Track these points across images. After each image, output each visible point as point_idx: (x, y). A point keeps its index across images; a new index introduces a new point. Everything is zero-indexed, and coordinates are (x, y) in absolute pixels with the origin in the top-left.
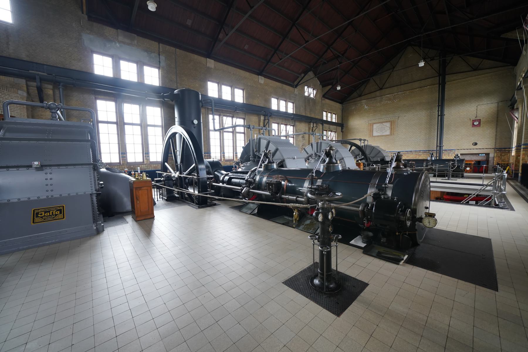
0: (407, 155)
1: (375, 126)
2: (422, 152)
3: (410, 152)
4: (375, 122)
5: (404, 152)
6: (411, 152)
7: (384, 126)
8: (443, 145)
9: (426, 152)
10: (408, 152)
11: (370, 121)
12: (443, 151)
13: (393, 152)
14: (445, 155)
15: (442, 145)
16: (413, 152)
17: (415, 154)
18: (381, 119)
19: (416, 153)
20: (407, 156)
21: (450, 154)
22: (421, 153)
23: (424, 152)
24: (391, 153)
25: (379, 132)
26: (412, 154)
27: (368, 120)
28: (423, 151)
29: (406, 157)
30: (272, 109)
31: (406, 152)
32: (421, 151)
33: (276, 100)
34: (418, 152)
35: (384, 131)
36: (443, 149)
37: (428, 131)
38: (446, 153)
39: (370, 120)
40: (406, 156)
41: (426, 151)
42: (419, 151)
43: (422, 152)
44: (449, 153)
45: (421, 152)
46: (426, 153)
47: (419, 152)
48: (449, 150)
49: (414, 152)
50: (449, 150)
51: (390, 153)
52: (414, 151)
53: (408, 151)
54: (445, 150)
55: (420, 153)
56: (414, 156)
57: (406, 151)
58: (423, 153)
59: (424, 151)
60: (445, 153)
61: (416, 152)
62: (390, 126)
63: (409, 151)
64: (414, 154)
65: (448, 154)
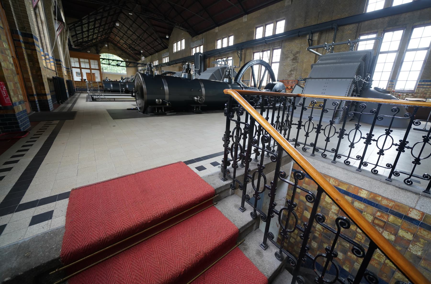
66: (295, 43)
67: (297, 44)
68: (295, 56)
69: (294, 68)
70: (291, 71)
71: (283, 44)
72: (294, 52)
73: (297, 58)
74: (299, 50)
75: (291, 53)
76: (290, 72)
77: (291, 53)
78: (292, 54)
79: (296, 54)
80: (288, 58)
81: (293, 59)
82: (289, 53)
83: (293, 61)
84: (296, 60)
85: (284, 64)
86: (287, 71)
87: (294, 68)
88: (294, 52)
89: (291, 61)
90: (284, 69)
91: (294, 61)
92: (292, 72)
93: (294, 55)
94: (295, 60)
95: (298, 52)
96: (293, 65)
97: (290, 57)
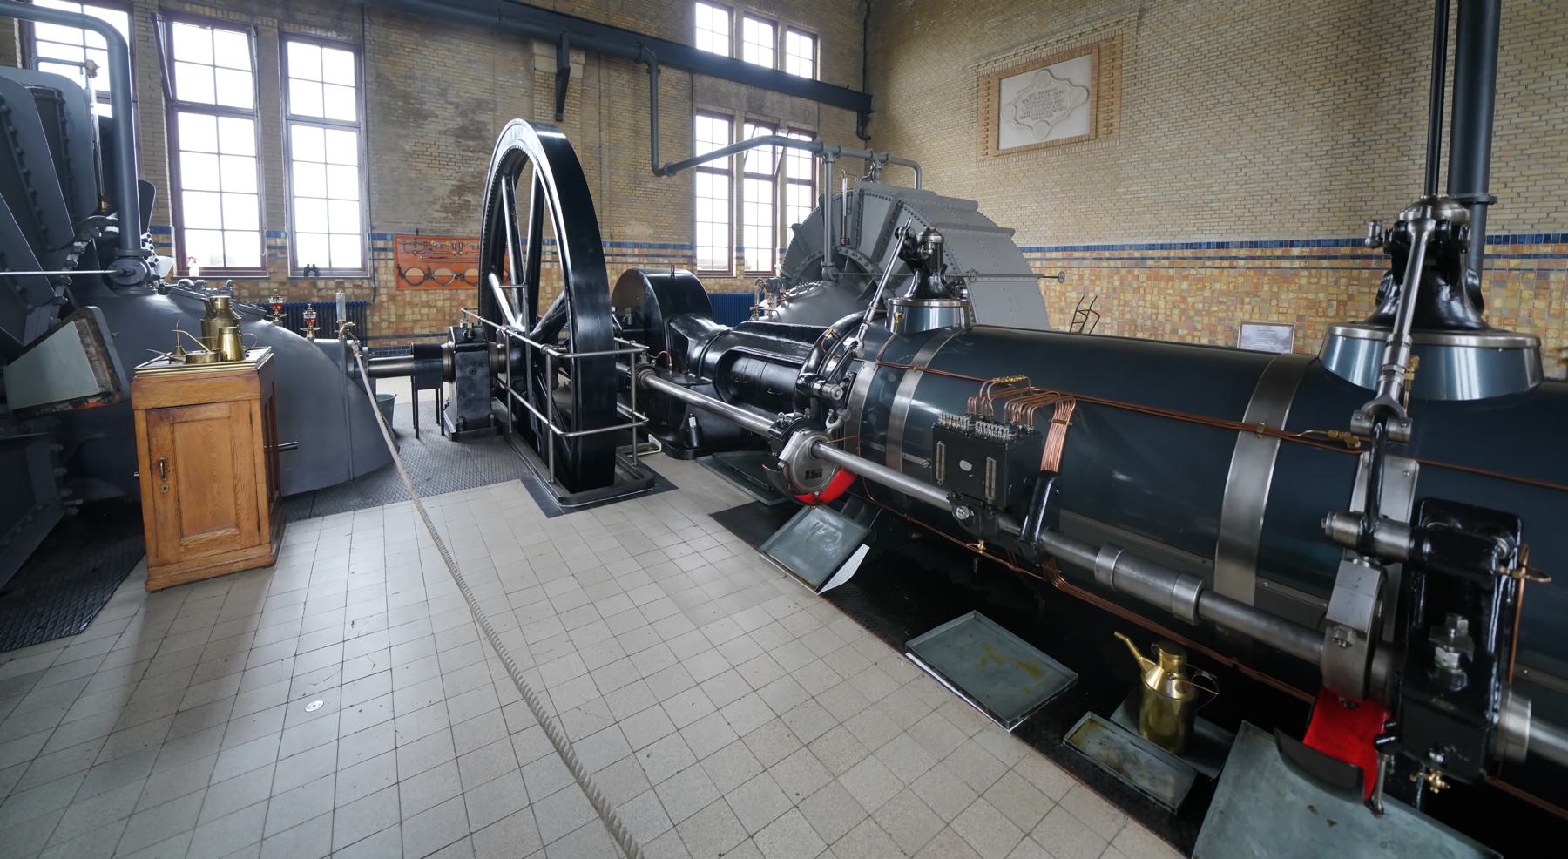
0: (1193, 272)
1: (1011, 89)
2: (1306, 252)
3: (1211, 252)
4: (1009, 63)
5: (1172, 253)
6: (1222, 252)
7: (1054, 84)
8: (1485, 189)
9: (1332, 251)
10: (1199, 253)
11: (982, 62)
12: (1488, 249)
13: (1105, 248)
14: (1500, 283)
15: (1479, 195)
16: (1234, 252)
17: (1251, 264)
18: (1038, 38)
19: (1259, 263)
20: (1201, 280)
21: (1553, 276)
22: (1297, 264)
23: (1316, 251)
24: (1095, 254)
25: (1032, 123)
26: (1226, 263)
27: (978, 54)
28: (1307, 243)
29: (1185, 286)
30: (786, 74)
31: (1188, 253)
32: (1291, 244)
33: (767, 29)
34: (1268, 252)
35: (1056, 114)
36: (1491, 231)
37: (1351, 85)
38: (1514, 263)
39: (984, 57)
40: (1185, 278)
41: (1337, 243)
42: (1281, 244)
43: (1306, 252)
44: (1551, 263)
45: (1296, 251)
46: (1336, 263)
47: (1278, 252)
48: (1547, 239)
49: (1243, 252)
50: (1547, 239)
51: (1087, 254)
52: (1241, 245)
53: (1198, 246)
54: (1506, 240)
55: (1286, 264)
56: (1241, 280)
57: (1187, 246)
58: (1314, 263)
59: (1319, 243)
60: (1499, 263)
61: (1259, 252)
62: (1087, 83)
63: (1209, 245)
64: (1241, 263)
65: (1532, 276)
66: (459, 53)
67: (469, 61)
68: (473, 122)
69: (475, 177)
70: (460, 190)
71: (367, 25)
72: (459, 97)
73: (486, 133)
74: (485, 96)
75: (443, 93)
76: (452, 193)
77: (441, 95)
78: (451, 103)
79: (473, 112)
80: (425, 118)
81: (462, 133)
82: (429, 92)
83: (463, 142)
84: (481, 138)
85: (407, 148)
86: (430, 190)
87: (475, 177)
88: (459, 97)
89: (452, 140)
90: (413, 174)
91: (471, 143)
92: (469, 197)
93: (463, 114)
94: (474, 138)
95: (480, 105)
96: (464, 160)
97: (437, 117)
